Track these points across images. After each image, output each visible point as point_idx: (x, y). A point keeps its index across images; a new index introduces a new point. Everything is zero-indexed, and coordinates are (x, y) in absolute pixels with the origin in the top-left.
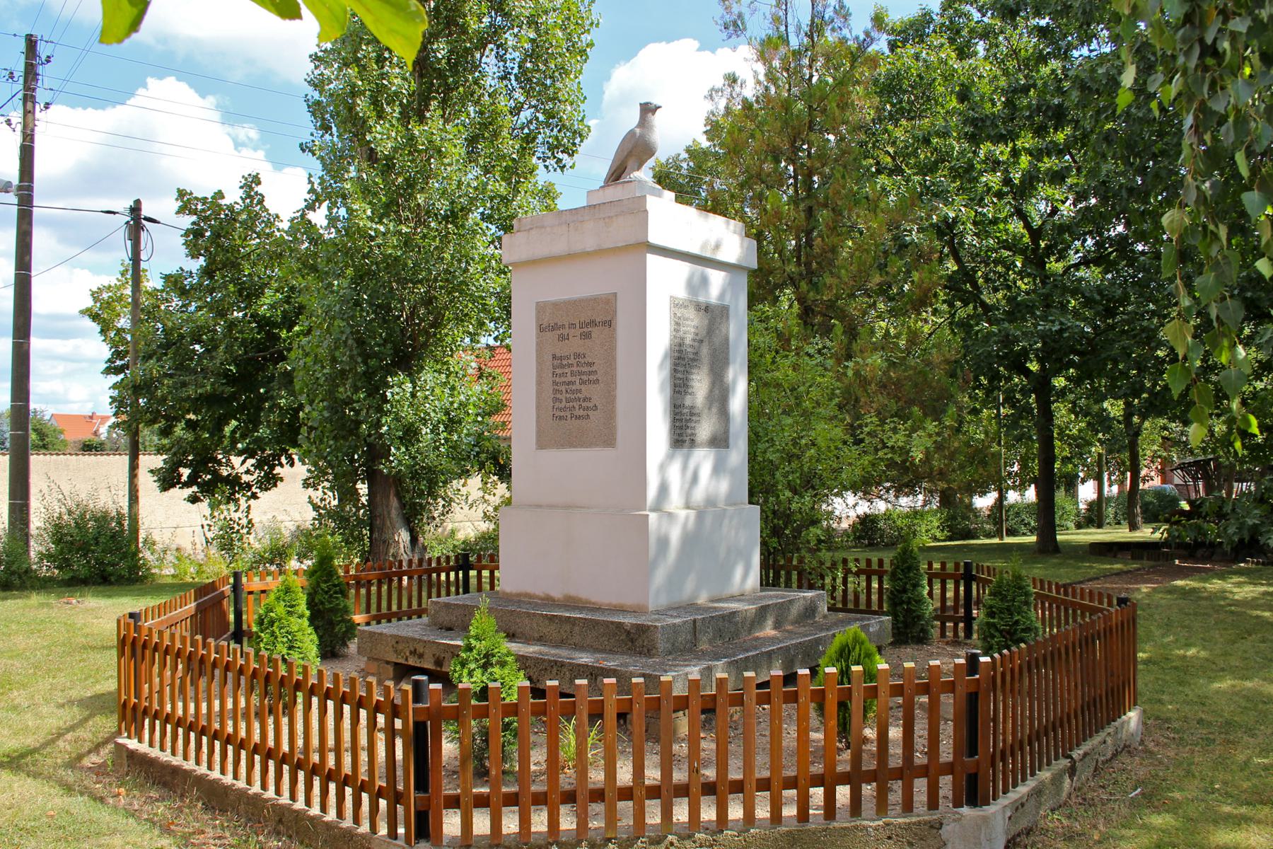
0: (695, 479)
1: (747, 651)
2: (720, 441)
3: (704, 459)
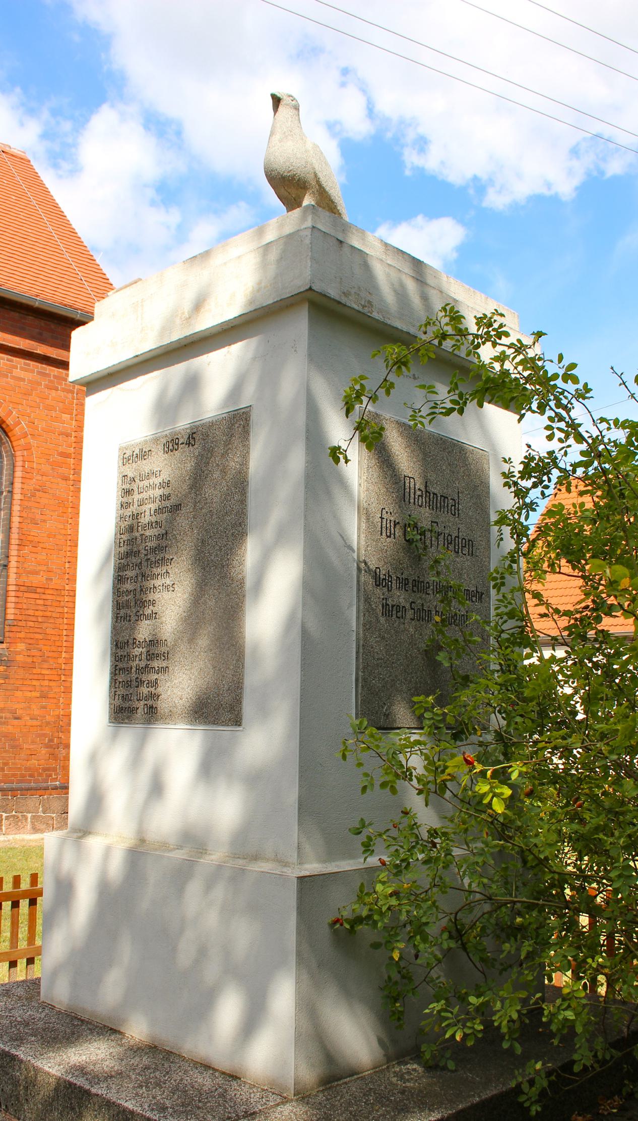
0: (157, 788)
1: (358, 1078)
2: (219, 709)
3: (178, 745)
